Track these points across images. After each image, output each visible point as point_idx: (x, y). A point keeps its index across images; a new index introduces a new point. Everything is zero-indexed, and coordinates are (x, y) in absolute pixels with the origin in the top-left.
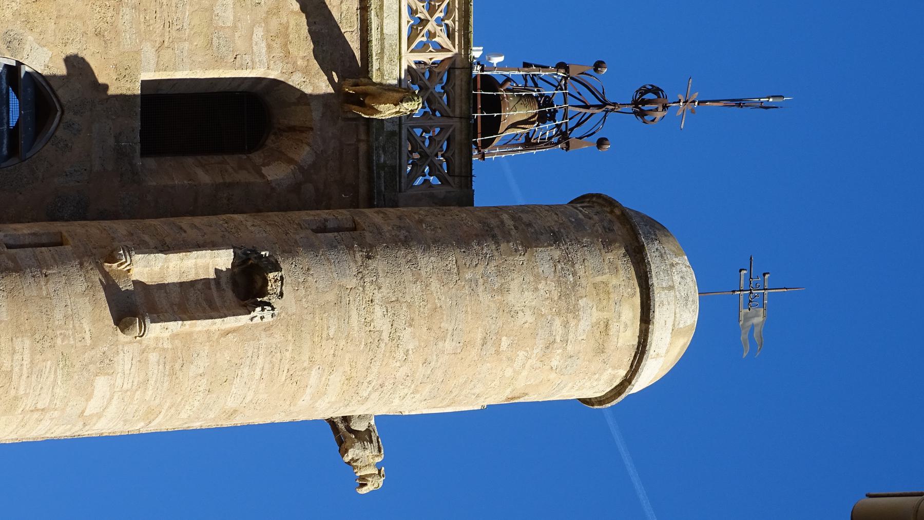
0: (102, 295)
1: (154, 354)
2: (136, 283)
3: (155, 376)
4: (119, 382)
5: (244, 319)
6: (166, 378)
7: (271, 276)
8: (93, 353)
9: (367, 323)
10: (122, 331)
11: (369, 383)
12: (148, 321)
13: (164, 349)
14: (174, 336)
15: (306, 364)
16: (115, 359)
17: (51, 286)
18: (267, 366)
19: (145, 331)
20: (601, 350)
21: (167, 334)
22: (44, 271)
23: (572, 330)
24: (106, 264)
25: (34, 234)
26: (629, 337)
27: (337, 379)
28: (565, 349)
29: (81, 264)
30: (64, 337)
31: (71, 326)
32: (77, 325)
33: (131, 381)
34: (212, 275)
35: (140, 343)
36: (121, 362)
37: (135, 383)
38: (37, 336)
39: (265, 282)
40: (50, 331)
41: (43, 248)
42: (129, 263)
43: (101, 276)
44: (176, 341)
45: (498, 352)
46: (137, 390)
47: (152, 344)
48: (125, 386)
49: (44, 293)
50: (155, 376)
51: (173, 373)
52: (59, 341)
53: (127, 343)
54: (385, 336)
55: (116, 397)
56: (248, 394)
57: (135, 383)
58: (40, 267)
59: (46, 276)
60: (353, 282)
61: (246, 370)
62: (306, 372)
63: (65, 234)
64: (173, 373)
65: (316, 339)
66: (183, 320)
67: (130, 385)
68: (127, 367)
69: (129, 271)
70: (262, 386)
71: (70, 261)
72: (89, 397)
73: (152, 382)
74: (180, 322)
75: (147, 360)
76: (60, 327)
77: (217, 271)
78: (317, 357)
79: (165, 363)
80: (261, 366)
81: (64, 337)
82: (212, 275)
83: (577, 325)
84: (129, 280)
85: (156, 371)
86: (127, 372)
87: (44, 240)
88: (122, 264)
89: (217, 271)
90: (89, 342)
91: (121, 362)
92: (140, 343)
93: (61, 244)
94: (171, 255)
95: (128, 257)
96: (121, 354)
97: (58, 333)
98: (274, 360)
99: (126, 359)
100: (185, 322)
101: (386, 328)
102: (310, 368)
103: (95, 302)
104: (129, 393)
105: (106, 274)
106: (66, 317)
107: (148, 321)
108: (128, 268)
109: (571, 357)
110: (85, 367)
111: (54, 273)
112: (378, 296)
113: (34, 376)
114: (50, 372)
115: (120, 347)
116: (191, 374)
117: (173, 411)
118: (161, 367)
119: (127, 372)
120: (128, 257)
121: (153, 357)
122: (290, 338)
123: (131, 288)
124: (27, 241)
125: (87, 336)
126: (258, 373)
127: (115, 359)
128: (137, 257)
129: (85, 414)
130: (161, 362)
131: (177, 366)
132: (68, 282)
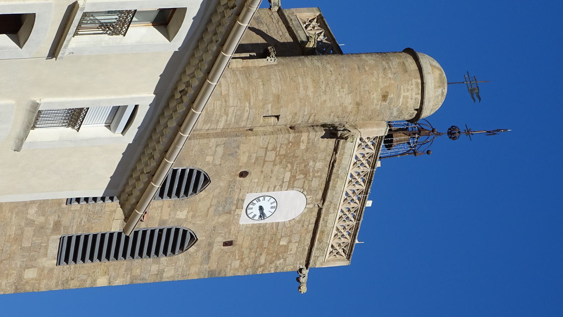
20: (406, 71)
23: (391, 64)
26: (414, 66)
27: (309, 80)
28: (391, 70)
33: (233, 80)
45: (365, 71)
46: (236, 83)
48: (232, 81)
50: (241, 78)
51: (247, 77)
55: (230, 86)
56: (279, 86)
70: (282, 82)
73: (241, 80)
80: (278, 75)
83: (392, 63)
86: (230, 77)
102: (297, 76)
104: (234, 84)
109: (395, 73)
117: (254, 94)
119: (230, 77)
121: (238, 73)
122: (285, 67)
126: (279, 78)
129: (223, 94)
130: (241, 73)
131: (248, 75)
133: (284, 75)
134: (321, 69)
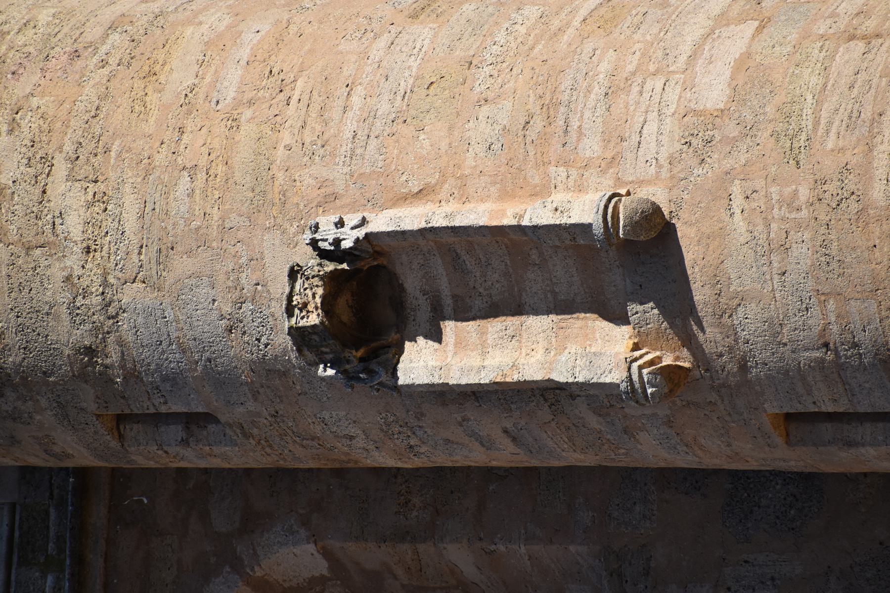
0: (700, 294)
1: (588, 154)
2: (619, 318)
3: (591, 103)
4: (673, 94)
5: (380, 223)
6: (565, 97)
7: (314, 319)
8: (728, 164)
9: (100, 200)
10: (656, 210)
11: (104, 63)
12: (598, 229)
13: (566, 164)
14: (541, 192)
15: (248, 113)
16: (678, 146)
17: (815, 320)
18: (336, 114)
19: (606, 207)
21: (558, 198)
22: (830, 356)
24: (687, 365)
25: (850, 444)
29: (744, 367)
30: (791, 203)
31: (774, 226)
32: (760, 228)
33: (646, 95)
34: (449, 327)
35: (618, 181)
36: (665, 139)
37: (636, 89)
38: (854, 207)
39: (327, 306)
40: (823, 217)
41: (830, 408)
42: (635, 365)
43: (701, 337)
44: (537, 180)
46: (634, 74)
47: (592, 176)
48: (659, 85)
49: (831, 305)
50: (591, 103)
52: (804, 193)
53: (649, 182)
54: (61, 168)
55: (683, 59)
56: (381, 53)
57: (636, 89)
58: (839, 366)
59: (826, 345)
60: (129, 295)
61: (384, 108)
62: (249, 95)
63: (780, 441)
64: (549, 108)
65: (220, 169)
66: (519, 228)
67: (648, 86)
68: (651, 128)
69: (636, 347)
70: (348, 70)
71: (768, 377)
72: (742, 63)
73: (598, 91)
74: (525, 222)
75: (606, 141)
76: (799, 226)
77: (436, 336)
78: (220, 129)
79: (566, 132)
80: (350, 114)
81: (791, 203)
82: (449, 327)
84: (638, 326)
85: (587, 114)
87: (826, 429)
88: (651, 363)
89: (436, 336)
90: (736, 189)
91: (665, 139)
92: (618, 181)
93: (789, 417)
94: (538, 377)
95: (635, 377)
96: (663, 157)
97: (804, 213)
98: (318, 128)
99: (653, 145)
100: (514, 222)
101: (58, 185)
102: (238, 103)
103: (716, 281)
104: (652, 68)
105: (689, 341)
106: (785, 249)
107: (598, 229)
108: (637, 354)
110: (749, 131)
111: (806, 349)
112: (73, 261)
113: (867, 114)
114: (830, 123)
115: (665, 174)
116: (508, 104)
117: (556, 23)
118: (575, 124)
119: (653, 116)
120: (635, 377)
122: (280, 176)
123: (633, 308)
124: (867, 430)
125: (738, 202)
126: (356, 100)
127: (678, 146)
128: (615, 376)
129: (756, 23)
130: (573, 135)
131: (538, 123)
132: (774, 327)
133: (314, 113)
134: (66, 148)
